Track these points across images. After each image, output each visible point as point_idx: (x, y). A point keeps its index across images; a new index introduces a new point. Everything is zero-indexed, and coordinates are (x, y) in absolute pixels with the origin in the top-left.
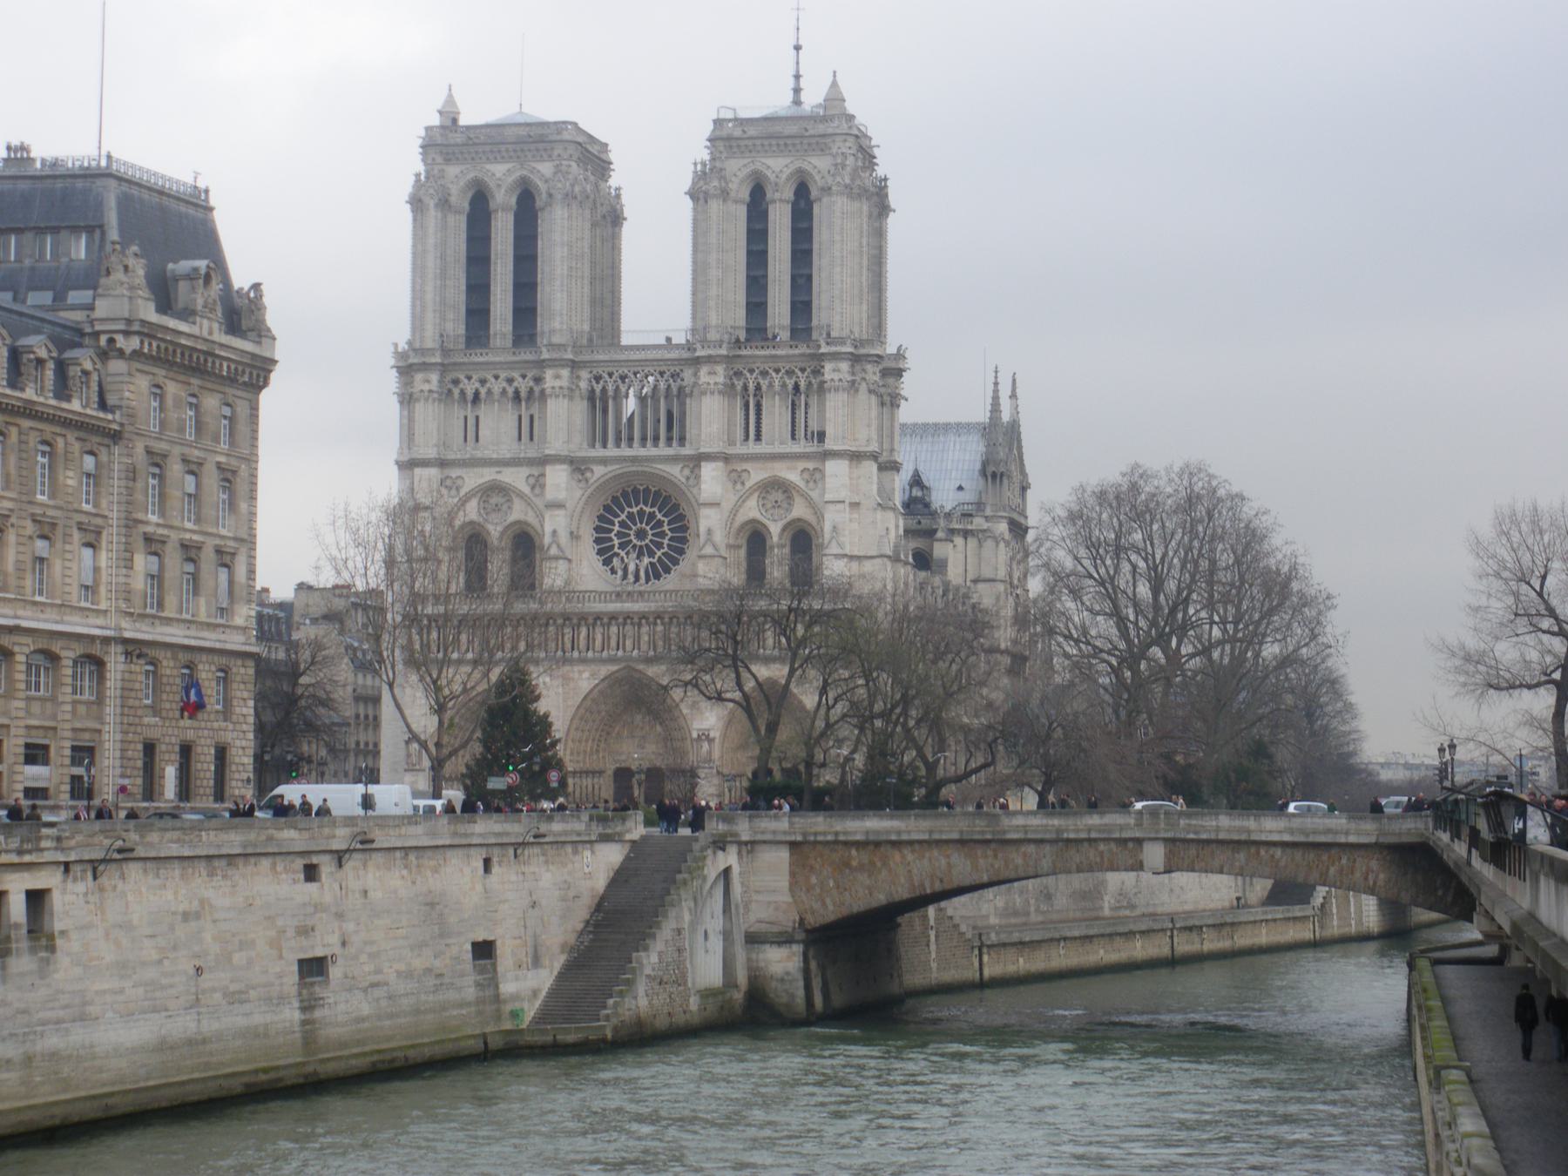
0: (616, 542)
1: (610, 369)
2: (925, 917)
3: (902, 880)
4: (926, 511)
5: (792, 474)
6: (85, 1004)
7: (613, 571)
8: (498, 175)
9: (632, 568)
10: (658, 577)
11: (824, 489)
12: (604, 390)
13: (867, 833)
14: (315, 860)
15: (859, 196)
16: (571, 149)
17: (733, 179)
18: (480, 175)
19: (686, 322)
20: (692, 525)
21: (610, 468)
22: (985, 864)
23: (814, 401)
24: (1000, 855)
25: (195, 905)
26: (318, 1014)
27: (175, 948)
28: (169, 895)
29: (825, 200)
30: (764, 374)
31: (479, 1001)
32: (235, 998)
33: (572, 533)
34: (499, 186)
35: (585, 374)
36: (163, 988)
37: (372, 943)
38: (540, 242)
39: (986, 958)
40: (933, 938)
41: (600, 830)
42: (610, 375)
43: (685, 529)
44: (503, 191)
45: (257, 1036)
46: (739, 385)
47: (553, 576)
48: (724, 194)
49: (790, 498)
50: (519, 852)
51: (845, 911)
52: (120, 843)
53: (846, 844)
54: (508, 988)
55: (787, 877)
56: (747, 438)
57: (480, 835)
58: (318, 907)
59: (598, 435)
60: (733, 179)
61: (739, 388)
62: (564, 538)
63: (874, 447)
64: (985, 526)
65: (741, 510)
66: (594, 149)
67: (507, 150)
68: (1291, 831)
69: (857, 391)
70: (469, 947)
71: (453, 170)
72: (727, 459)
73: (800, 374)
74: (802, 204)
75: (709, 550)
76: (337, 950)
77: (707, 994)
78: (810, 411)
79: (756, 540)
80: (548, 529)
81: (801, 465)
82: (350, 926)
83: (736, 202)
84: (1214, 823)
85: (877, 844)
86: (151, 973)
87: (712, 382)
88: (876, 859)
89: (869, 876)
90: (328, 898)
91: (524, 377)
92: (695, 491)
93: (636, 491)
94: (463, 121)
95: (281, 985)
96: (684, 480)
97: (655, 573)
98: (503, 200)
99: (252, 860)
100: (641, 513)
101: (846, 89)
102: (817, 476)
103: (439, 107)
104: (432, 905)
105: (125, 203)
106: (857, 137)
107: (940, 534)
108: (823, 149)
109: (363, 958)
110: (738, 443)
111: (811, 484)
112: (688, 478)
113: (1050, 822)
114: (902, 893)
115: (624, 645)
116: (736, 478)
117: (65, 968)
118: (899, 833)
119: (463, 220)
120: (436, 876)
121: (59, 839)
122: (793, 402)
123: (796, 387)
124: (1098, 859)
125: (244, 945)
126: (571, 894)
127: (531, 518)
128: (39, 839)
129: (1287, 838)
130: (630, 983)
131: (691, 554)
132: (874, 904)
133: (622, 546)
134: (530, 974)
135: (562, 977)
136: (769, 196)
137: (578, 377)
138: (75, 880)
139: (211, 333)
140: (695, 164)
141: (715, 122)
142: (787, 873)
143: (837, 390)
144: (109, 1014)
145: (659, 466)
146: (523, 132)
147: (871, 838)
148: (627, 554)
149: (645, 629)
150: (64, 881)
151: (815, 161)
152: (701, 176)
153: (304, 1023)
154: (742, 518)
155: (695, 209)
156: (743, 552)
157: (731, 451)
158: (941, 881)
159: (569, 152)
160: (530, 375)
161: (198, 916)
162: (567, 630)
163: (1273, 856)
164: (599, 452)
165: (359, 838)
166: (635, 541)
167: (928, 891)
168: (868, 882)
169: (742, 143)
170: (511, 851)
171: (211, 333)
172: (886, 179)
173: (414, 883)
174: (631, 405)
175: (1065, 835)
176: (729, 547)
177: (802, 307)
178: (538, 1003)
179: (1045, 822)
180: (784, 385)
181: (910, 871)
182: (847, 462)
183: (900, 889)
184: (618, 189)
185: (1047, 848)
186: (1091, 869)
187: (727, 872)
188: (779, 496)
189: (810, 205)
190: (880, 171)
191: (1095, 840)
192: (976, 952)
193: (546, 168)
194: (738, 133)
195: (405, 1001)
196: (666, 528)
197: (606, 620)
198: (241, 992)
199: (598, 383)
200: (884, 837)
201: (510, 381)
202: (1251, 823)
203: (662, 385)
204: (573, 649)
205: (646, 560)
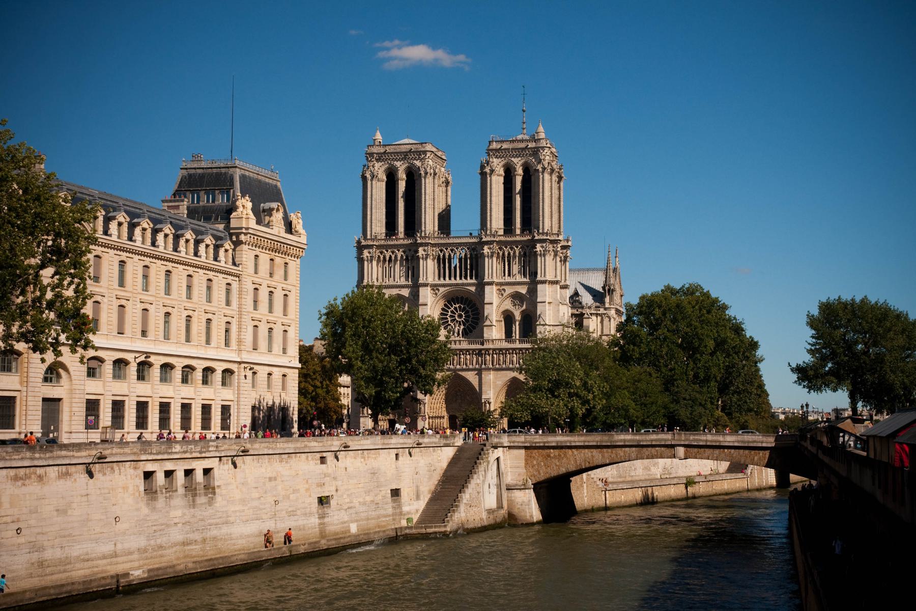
2: (582, 478)
3: (573, 463)
4: (580, 306)
6: (228, 517)
9: (456, 330)
12: (444, 256)
13: (557, 442)
14: (324, 455)
19: (479, 227)
21: (447, 288)
22: (608, 454)
23: (532, 259)
24: (614, 452)
25: (274, 475)
26: (326, 520)
27: (266, 492)
28: (263, 470)
31: (393, 515)
32: (292, 514)
36: (261, 509)
37: (348, 490)
38: (416, 194)
39: (607, 496)
40: (585, 487)
41: (445, 442)
43: (478, 314)
45: (300, 530)
48: (492, 171)
51: (548, 476)
52: (243, 448)
54: (405, 509)
56: (504, 275)
57: (394, 444)
58: (326, 475)
59: (441, 274)
64: (605, 312)
68: (738, 442)
70: (390, 492)
72: (497, 284)
76: (334, 493)
77: (490, 511)
78: (531, 264)
79: (508, 318)
82: (339, 483)
84: (705, 438)
86: (255, 503)
90: (330, 471)
91: (410, 250)
95: (310, 508)
98: (402, 175)
99: (298, 455)
104: (374, 473)
105: (243, 177)
106: (550, 148)
107: (586, 316)
109: (345, 496)
114: (572, 468)
116: (501, 292)
117: (219, 501)
118: (570, 442)
119: (384, 184)
120: (376, 461)
121: (217, 447)
123: (525, 254)
125: (295, 491)
126: (433, 468)
128: (209, 447)
129: (736, 444)
130: (457, 506)
132: (561, 473)
133: (452, 321)
134: (415, 503)
135: (428, 504)
138: (224, 464)
139: (279, 233)
144: (238, 521)
146: (409, 147)
147: (559, 445)
148: (454, 324)
150: (219, 465)
153: (320, 524)
154: (502, 309)
156: (503, 323)
158: (589, 463)
160: (412, 250)
161: (275, 479)
163: (730, 452)
164: (442, 281)
165: (343, 446)
171: (279, 233)
173: (366, 464)
174: (455, 262)
178: (418, 515)
186: (652, 458)
187: (498, 459)
189: (530, 177)
192: (604, 492)
195: (362, 515)
198: (293, 511)
201: (404, 252)
202: (721, 438)
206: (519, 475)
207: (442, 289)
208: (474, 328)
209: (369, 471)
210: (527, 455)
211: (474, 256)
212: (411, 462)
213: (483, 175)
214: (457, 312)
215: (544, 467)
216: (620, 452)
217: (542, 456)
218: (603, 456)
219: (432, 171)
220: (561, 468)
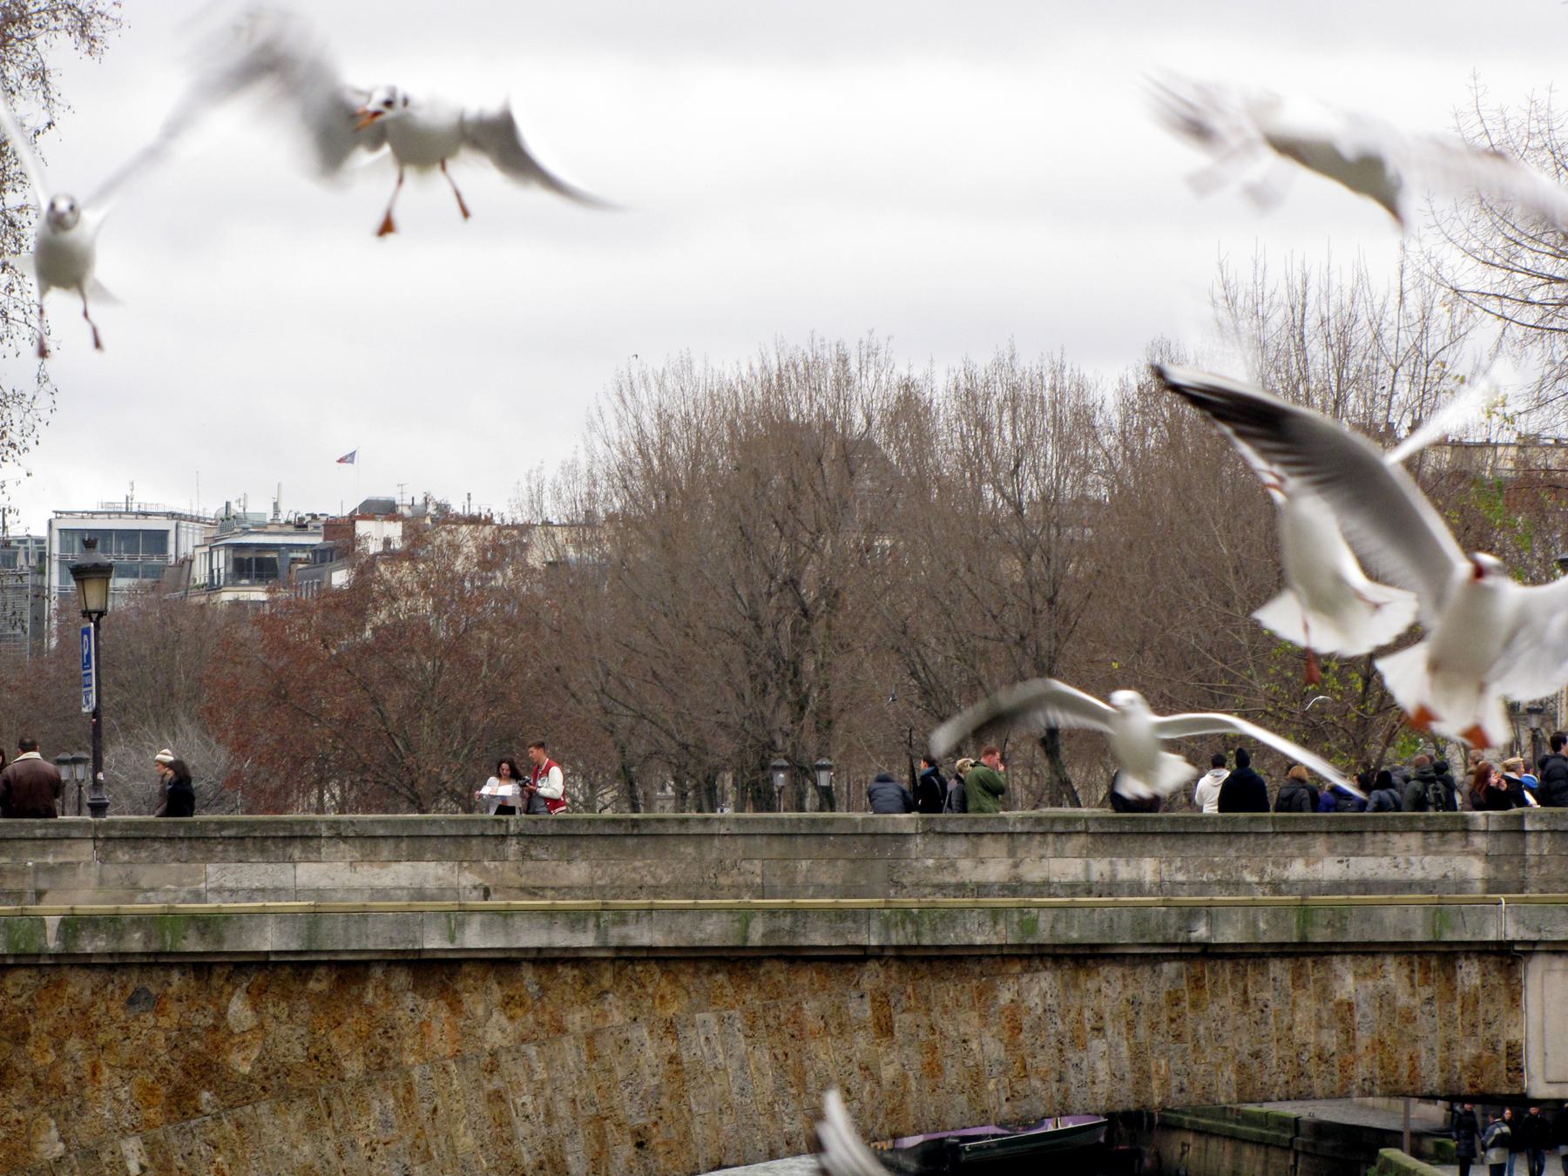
3: (467, 1141)
13: (314, 917)
24: (903, 1021)
53: (201, 967)
89: (311, 1123)
113: (1125, 871)
118: (458, 917)
124: (1331, 1040)
147: (341, 940)
175: (1201, 932)
179: (1100, 868)
181: (497, 1097)
191: (1324, 952)
200: (378, 938)
216: (968, 1022)
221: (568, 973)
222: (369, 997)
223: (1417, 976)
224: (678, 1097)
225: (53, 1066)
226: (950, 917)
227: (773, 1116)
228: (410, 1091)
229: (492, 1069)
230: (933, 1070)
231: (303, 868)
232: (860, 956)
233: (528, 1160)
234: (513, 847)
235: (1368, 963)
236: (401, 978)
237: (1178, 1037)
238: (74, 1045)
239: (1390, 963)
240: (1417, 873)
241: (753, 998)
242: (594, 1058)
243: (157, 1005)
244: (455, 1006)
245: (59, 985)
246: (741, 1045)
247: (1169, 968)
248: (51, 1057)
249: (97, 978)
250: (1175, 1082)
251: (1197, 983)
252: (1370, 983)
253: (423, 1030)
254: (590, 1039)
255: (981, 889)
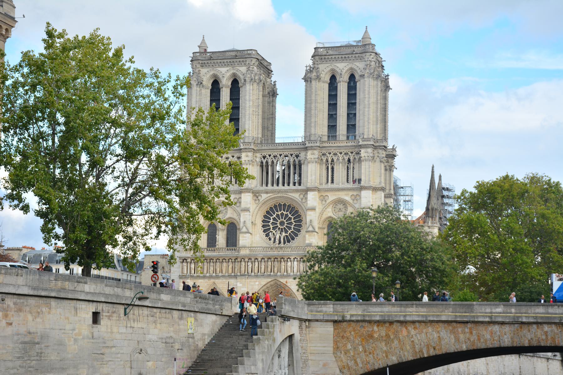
0: (271, 227)
1: (269, 153)
3: (408, 348)
5: (347, 197)
7: (270, 239)
8: (223, 73)
9: (278, 237)
10: (289, 241)
11: (360, 203)
12: (267, 162)
15: (377, 78)
16: (254, 61)
17: (323, 72)
18: (216, 73)
20: (304, 220)
21: (269, 195)
23: (356, 166)
24: (474, 332)
29: (362, 81)
30: (335, 154)
33: (252, 222)
34: (223, 77)
35: (258, 155)
42: (270, 156)
43: (300, 221)
44: (225, 79)
46: (324, 159)
47: (243, 240)
48: (318, 78)
49: (346, 208)
50: (128, 310)
51: (370, 368)
53: (370, 322)
55: (332, 345)
60: (323, 72)
61: (324, 161)
62: (249, 224)
63: (383, 185)
65: (325, 213)
66: (265, 64)
67: (227, 62)
69: (375, 161)
71: (204, 71)
72: (319, 190)
73: (350, 154)
74: (352, 84)
75: (311, 229)
78: (355, 171)
80: (242, 220)
81: (351, 193)
83: (324, 82)
85: (391, 323)
87: (313, 158)
88: (390, 333)
89: (386, 345)
91: (233, 157)
92: (305, 204)
93: (280, 205)
94: (208, 51)
96: (300, 200)
97: (288, 240)
100: (282, 214)
101: (371, 34)
102: (358, 197)
103: (199, 44)
108: (361, 59)
110: (324, 184)
111: (355, 201)
112: (302, 199)
115: (274, 270)
116: (323, 199)
119: (208, 92)
122: (347, 166)
123: (349, 160)
124: (544, 337)
127: (235, 216)
131: (303, 231)
133: (274, 228)
136: (338, 79)
137: (256, 157)
140: (306, 67)
141: (315, 48)
142: (332, 342)
143: (366, 160)
145: (290, 194)
146: (233, 54)
149: (283, 263)
151: (357, 64)
152: (310, 71)
154: (324, 216)
155: (306, 86)
157: (320, 187)
159: (253, 62)
162: (250, 264)
166: (279, 226)
167: (426, 356)
168: (385, 348)
169: (326, 57)
170: (122, 311)
172: (388, 76)
175: (520, 320)
176: (319, 228)
177: (351, 127)
180: (344, 159)
181: (413, 341)
182: (371, 192)
183: (406, 353)
184: (275, 82)
185: (507, 328)
187: (291, 337)
188: (341, 206)
189: (355, 83)
190: (386, 72)
191: (541, 323)
193: (243, 69)
194: (325, 53)
196: (293, 221)
197: (266, 259)
199: (264, 159)
203: (292, 160)
204: (252, 272)
205: (284, 234)
206: (324, 365)
207: (264, 196)
208: (297, 235)
209: (16, 338)
210: (336, 335)
211: (297, 163)
212: (130, 330)
213: (307, 79)
214: (279, 219)
215: (363, 355)
216: (484, 333)
217: (360, 336)
218: (457, 339)
219: (257, 78)
220: (390, 356)
221: (423, 324)
222: (394, 327)
223: (558, 328)
224: (440, 342)
225: (349, 336)
226: (478, 317)
227: (454, 345)
228: (400, 340)
229: (412, 337)
230: (479, 339)
231: (384, 308)
232: (467, 322)
233: (417, 351)
234: (414, 306)
235: (549, 325)
236: (399, 324)
237: (518, 336)
238: (353, 333)
239: (553, 326)
240: (557, 312)
241: (451, 328)
242: (427, 336)
243: (364, 327)
244: (406, 328)
245: (350, 324)
246: (449, 335)
247: (516, 325)
248: (349, 334)
249: (355, 323)
250: (518, 343)
251: (521, 328)
252: (550, 329)
253: (402, 332)
254: (426, 333)
255: (486, 313)
